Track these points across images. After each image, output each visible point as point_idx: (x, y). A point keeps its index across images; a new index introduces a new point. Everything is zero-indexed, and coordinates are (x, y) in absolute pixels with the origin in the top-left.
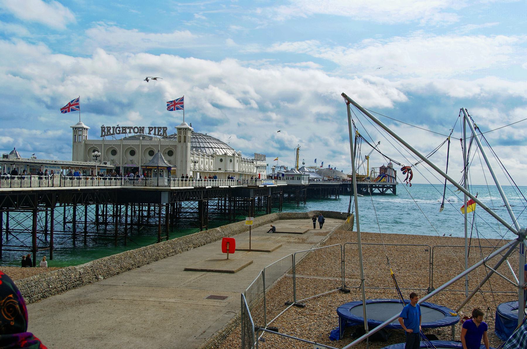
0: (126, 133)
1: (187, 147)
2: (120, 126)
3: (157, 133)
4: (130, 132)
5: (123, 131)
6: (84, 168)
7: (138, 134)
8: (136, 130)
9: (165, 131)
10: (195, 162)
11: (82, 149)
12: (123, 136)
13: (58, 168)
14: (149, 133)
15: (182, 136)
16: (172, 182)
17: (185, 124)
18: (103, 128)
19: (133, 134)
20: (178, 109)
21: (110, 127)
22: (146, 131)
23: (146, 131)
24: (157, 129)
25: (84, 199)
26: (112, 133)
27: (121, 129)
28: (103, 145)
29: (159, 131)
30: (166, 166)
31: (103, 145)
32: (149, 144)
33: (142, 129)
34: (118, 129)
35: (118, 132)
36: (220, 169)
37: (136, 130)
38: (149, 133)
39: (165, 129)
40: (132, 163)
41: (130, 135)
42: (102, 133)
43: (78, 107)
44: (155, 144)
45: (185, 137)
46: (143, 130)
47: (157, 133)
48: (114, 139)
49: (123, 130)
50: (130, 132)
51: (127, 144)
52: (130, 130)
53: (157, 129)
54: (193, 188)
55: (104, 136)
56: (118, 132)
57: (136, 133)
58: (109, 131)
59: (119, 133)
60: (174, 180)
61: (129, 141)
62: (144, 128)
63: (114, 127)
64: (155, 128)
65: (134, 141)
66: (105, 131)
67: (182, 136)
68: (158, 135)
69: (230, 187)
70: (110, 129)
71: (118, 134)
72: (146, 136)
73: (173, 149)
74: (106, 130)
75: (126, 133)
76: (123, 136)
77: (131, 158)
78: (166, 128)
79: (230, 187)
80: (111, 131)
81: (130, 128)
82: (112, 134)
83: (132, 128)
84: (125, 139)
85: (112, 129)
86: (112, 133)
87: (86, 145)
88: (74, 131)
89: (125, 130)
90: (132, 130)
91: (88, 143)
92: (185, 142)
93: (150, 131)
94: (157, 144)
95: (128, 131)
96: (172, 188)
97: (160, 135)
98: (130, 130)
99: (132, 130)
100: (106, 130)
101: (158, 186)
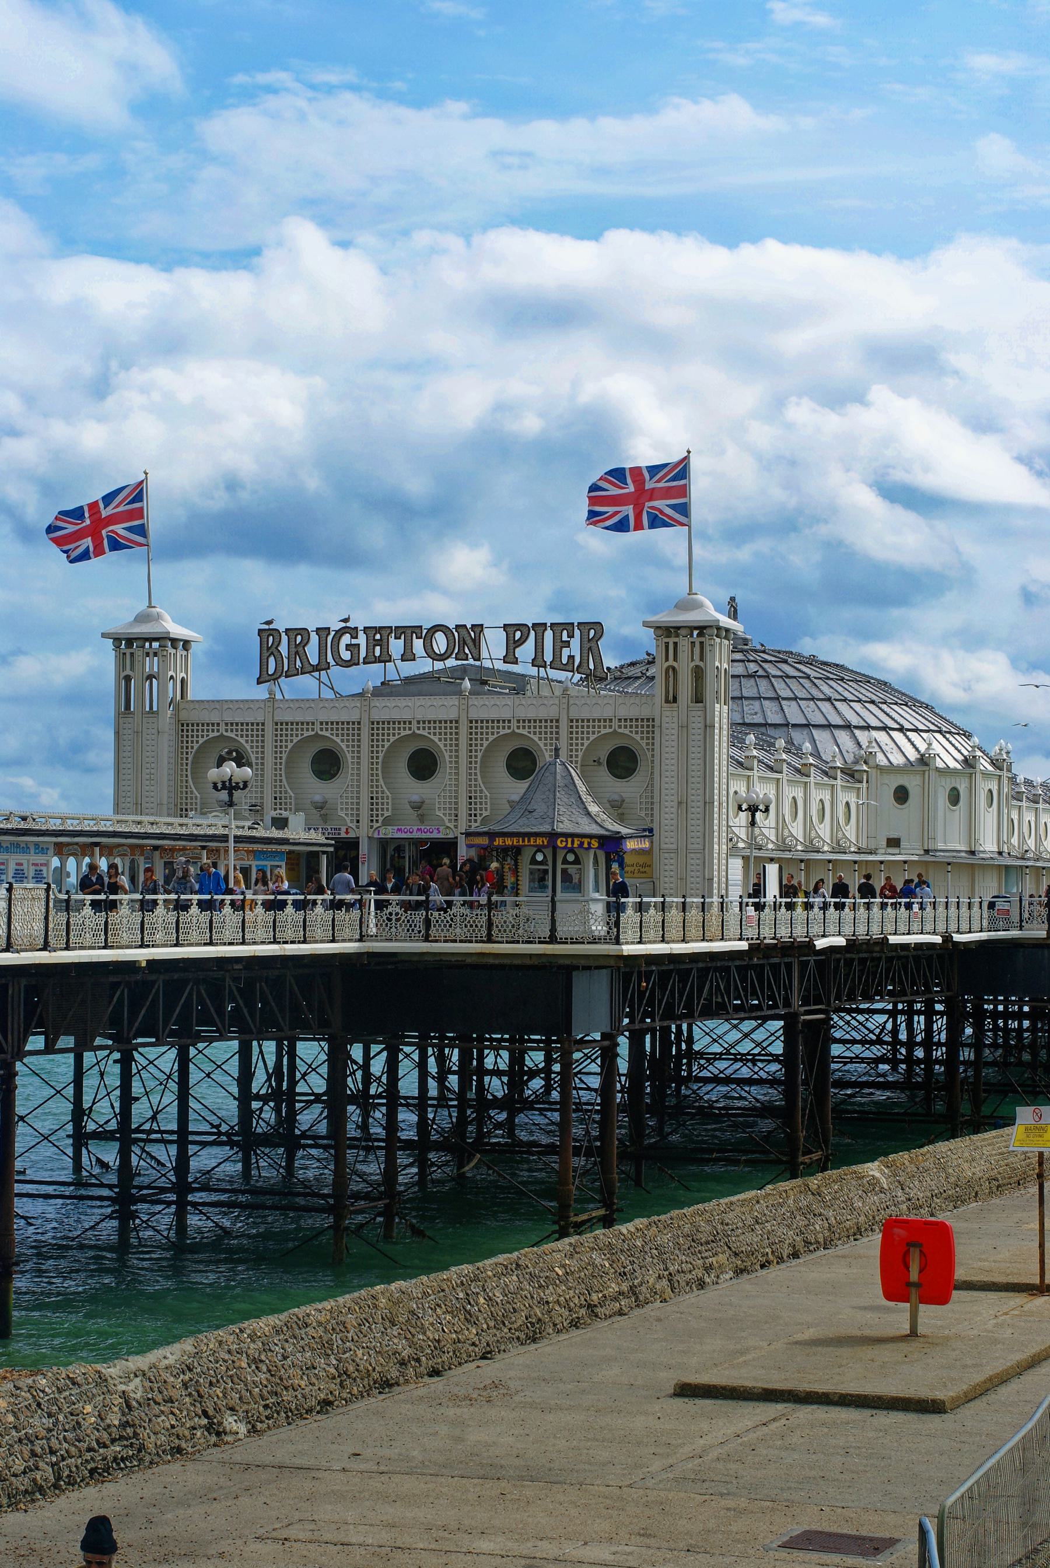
0: (385, 658)
1: (708, 727)
2: (359, 621)
3: (548, 657)
5: (370, 649)
6: (172, 850)
7: (451, 662)
8: (440, 643)
9: (590, 647)
10: (753, 809)
11: (163, 747)
12: (372, 675)
13: (40, 849)
15: (685, 667)
16: (629, 916)
17: (699, 606)
18: (268, 634)
19: (424, 665)
20: (656, 522)
21: (304, 632)
22: (494, 645)
23: (494, 645)
24: (549, 635)
25: (169, 1010)
26: (314, 661)
27: (362, 640)
29: (561, 645)
30: (595, 830)
32: (506, 714)
34: (346, 639)
35: (346, 655)
36: (894, 843)
37: (440, 643)
38: (510, 658)
40: (422, 818)
41: (409, 669)
42: (263, 665)
43: (142, 531)
44: (543, 714)
45: (699, 674)
46: (476, 643)
47: (548, 657)
48: (327, 694)
49: (372, 643)
50: (408, 656)
51: (396, 715)
52: (408, 646)
53: (549, 635)
54: (743, 945)
55: (275, 678)
56: (346, 655)
57: (442, 657)
60: (641, 908)
61: (402, 702)
62: (479, 628)
63: (322, 632)
64: (539, 627)
65: (426, 701)
66: (280, 651)
67: (685, 667)
69: (947, 938)
70: (306, 642)
71: (348, 664)
72: (493, 671)
73: (638, 740)
74: (284, 649)
75: (385, 658)
76: (372, 675)
77: (415, 790)
78: (598, 626)
79: (947, 938)
81: (407, 632)
82: (317, 668)
83: (416, 630)
84: (385, 689)
85: (314, 638)
86: (314, 661)
87: (184, 728)
88: (121, 660)
89: (383, 643)
90: (418, 644)
91: (194, 716)
92: (698, 698)
93: (512, 645)
94: (553, 713)
95: (396, 646)
96: (628, 949)
97: (569, 667)
98: (408, 646)
99: (418, 644)
100: (284, 649)
101: (553, 939)
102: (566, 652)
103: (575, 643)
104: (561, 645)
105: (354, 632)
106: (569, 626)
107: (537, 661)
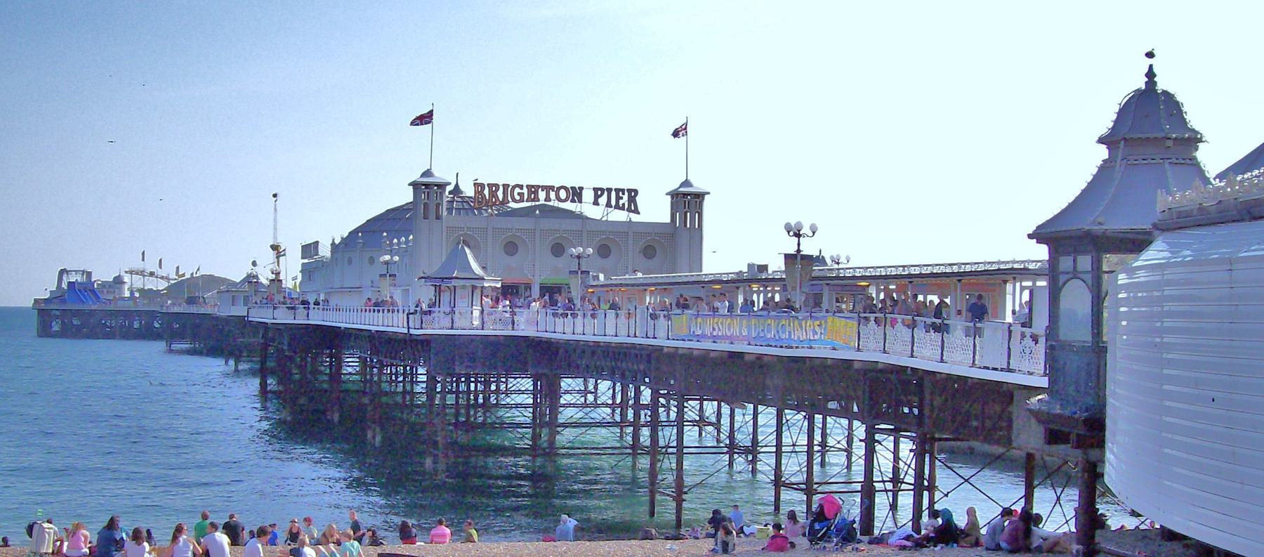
3: (613, 203)
4: (548, 199)
14: (596, 203)
21: (497, 186)
22: (588, 196)
23: (588, 196)
24: (613, 194)
27: (525, 191)
28: (490, 231)
29: (618, 198)
31: (490, 231)
33: (576, 194)
34: (517, 190)
35: (517, 198)
37: (563, 194)
38: (596, 203)
39: (633, 194)
47: (613, 203)
49: (530, 193)
53: (613, 194)
56: (517, 198)
58: (493, 194)
59: (522, 200)
62: (581, 189)
63: (506, 186)
64: (609, 190)
65: (568, 221)
68: (617, 207)
70: (497, 189)
78: (636, 192)
80: (500, 194)
81: (548, 189)
83: (552, 188)
89: (536, 193)
90: (553, 195)
93: (597, 197)
95: (542, 195)
97: (622, 208)
99: (553, 195)
102: (621, 202)
103: (626, 197)
104: (618, 198)
105: (521, 187)
106: (623, 191)
107: (608, 205)
